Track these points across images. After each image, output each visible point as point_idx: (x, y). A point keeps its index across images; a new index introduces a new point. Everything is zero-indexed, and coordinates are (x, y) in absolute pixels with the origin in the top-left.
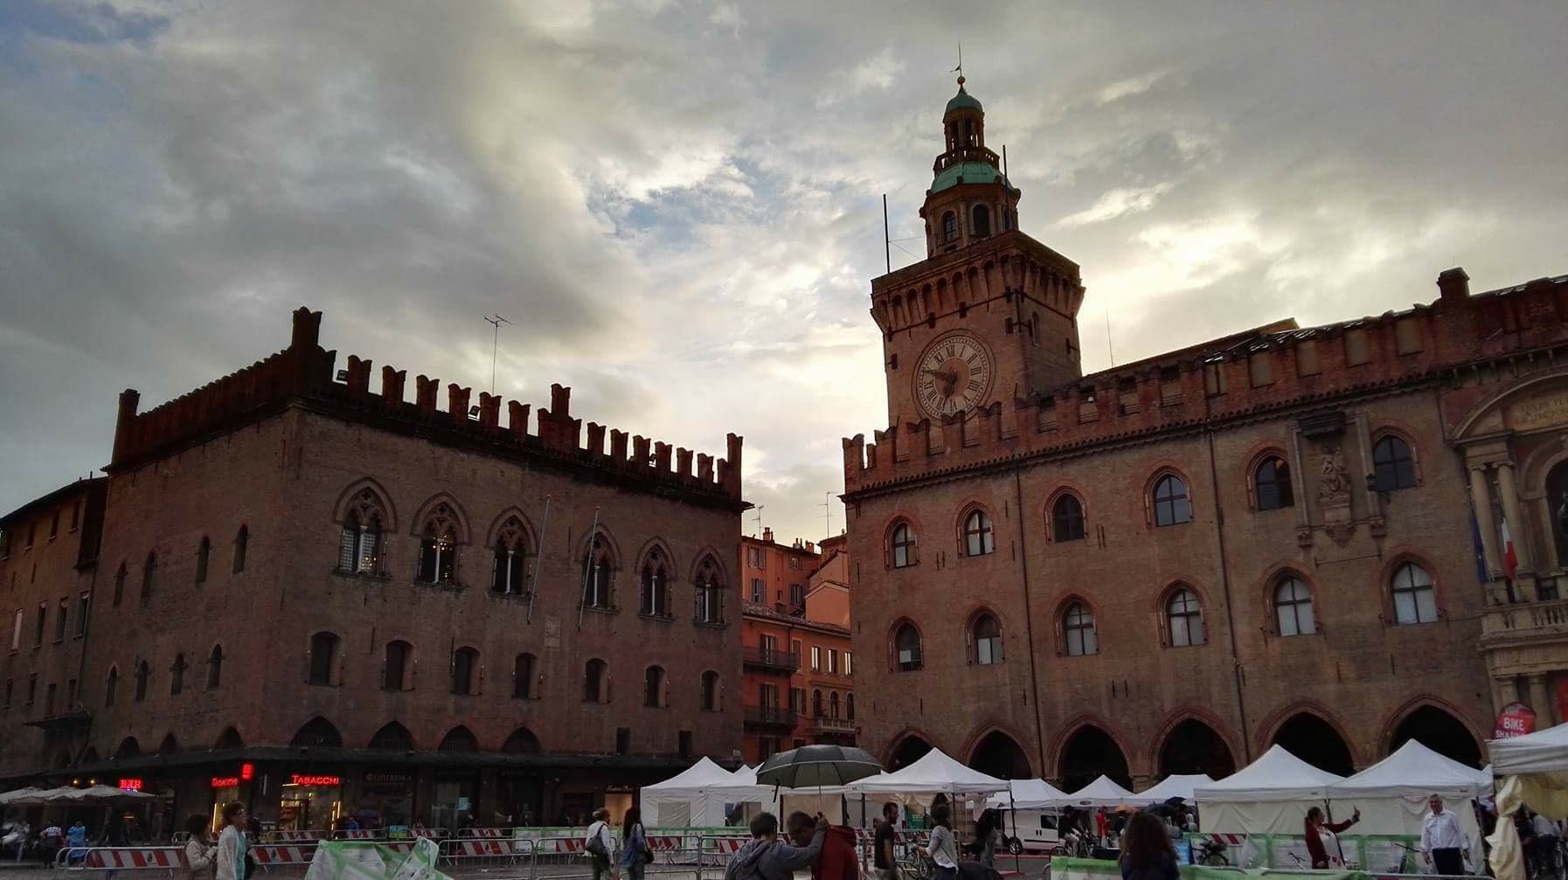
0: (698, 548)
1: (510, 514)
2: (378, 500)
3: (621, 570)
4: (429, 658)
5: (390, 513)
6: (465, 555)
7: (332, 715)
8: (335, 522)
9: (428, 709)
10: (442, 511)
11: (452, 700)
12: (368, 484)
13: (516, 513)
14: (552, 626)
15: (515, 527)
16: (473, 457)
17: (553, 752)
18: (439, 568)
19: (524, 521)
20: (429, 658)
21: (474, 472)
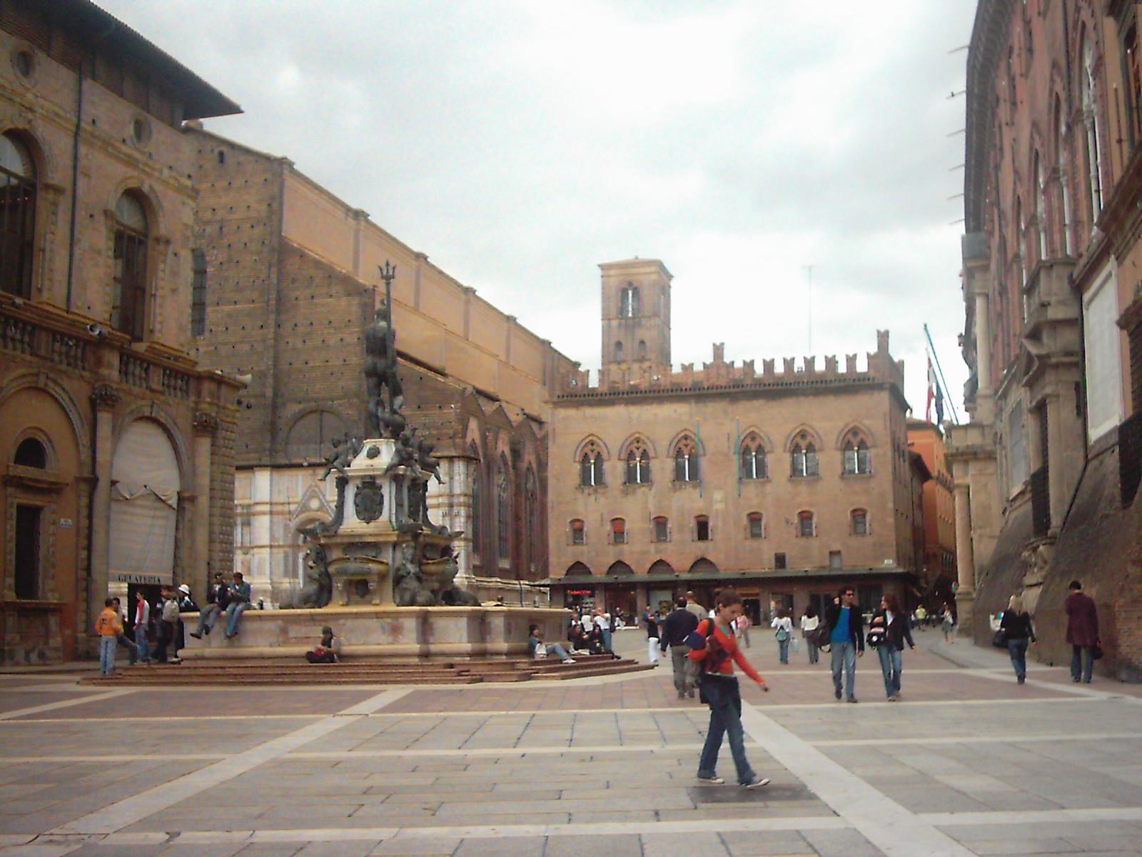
0: (841, 424)
1: (683, 434)
2: (598, 445)
3: (771, 452)
4: (637, 525)
5: (605, 451)
6: (654, 465)
7: (584, 560)
8: (575, 462)
9: (640, 554)
10: (638, 442)
11: (652, 548)
12: (590, 438)
13: (687, 433)
14: (718, 496)
15: (688, 441)
16: (655, 406)
17: (725, 570)
18: (637, 476)
19: (693, 436)
20: (637, 525)
21: (656, 415)
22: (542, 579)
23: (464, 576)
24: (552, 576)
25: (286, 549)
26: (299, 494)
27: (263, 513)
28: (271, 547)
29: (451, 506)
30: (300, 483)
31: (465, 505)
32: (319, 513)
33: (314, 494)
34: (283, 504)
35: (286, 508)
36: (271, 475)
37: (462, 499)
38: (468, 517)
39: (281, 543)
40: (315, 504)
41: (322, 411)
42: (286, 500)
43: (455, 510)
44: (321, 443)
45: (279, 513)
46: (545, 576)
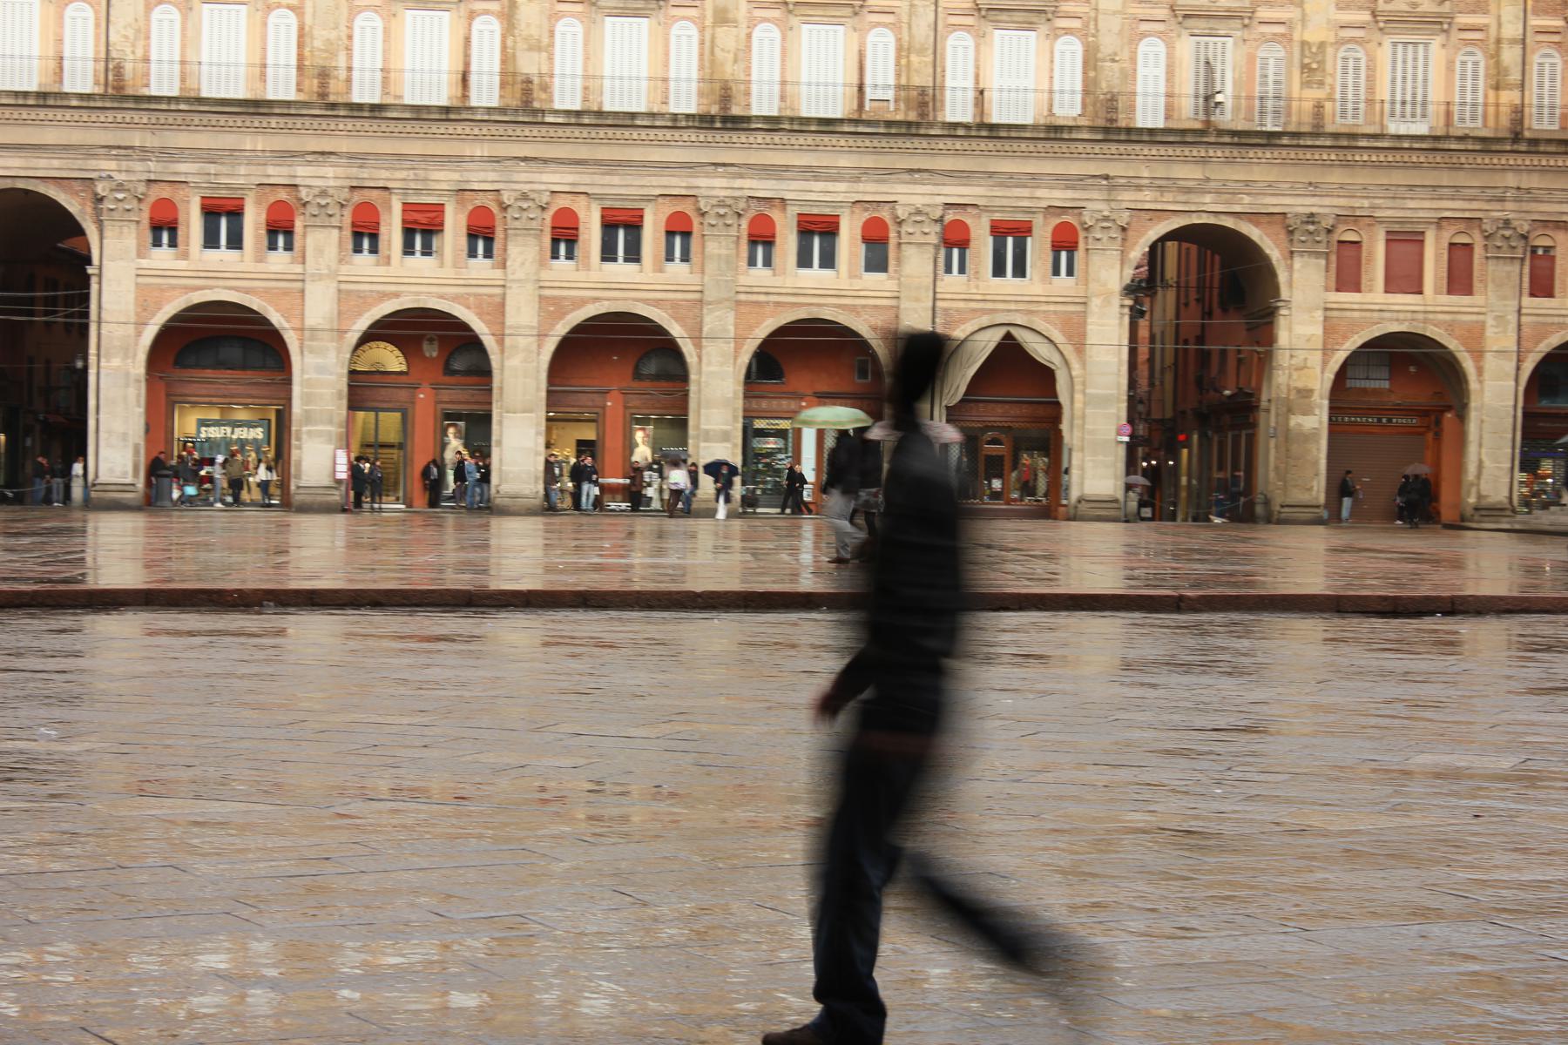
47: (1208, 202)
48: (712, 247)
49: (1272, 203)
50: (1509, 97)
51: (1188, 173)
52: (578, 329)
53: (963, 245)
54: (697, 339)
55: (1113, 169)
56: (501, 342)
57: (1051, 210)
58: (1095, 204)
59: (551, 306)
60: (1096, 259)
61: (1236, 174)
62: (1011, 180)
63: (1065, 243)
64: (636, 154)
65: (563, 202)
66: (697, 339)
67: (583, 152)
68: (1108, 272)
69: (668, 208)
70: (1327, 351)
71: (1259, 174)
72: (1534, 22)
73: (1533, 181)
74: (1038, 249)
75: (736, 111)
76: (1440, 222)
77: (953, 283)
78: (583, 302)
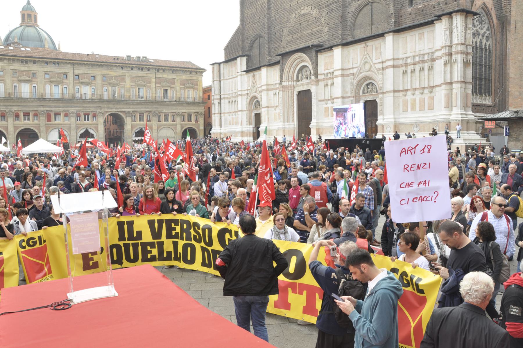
22: (500, 111)
23: (460, 112)
24: (512, 109)
25: (352, 99)
26: (358, 62)
27: (338, 76)
28: (343, 97)
29: (450, 55)
30: (359, 54)
31: (462, 53)
32: (369, 72)
33: (366, 60)
34: (350, 69)
35: (351, 71)
36: (342, 51)
37: (460, 48)
38: (466, 64)
39: (349, 95)
40: (367, 67)
41: (372, 3)
42: (351, 67)
43: (454, 57)
44: (372, 25)
45: (348, 75)
46: (502, 108)
47: (114, 110)
48: (41, 118)
49: (124, 110)
50: (154, 95)
51: (111, 106)
52: (20, 132)
53: (80, 116)
54: (40, 132)
55: (101, 105)
56: (8, 133)
57: (92, 111)
58: (99, 110)
59: (15, 127)
60: (99, 118)
61: (118, 106)
62: (86, 107)
63: (94, 116)
64: (28, 104)
65: (17, 112)
66: (40, 132)
67: (19, 104)
68: (101, 120)
69: (33, 113)
70: (132, 130)
71: (121, 106)
72: (157, 85)
73: (158, 107)
74: (90, 117)
75: (44, 97)
76: (146, 112)
77: (78, 122)
78: (21, 127)
